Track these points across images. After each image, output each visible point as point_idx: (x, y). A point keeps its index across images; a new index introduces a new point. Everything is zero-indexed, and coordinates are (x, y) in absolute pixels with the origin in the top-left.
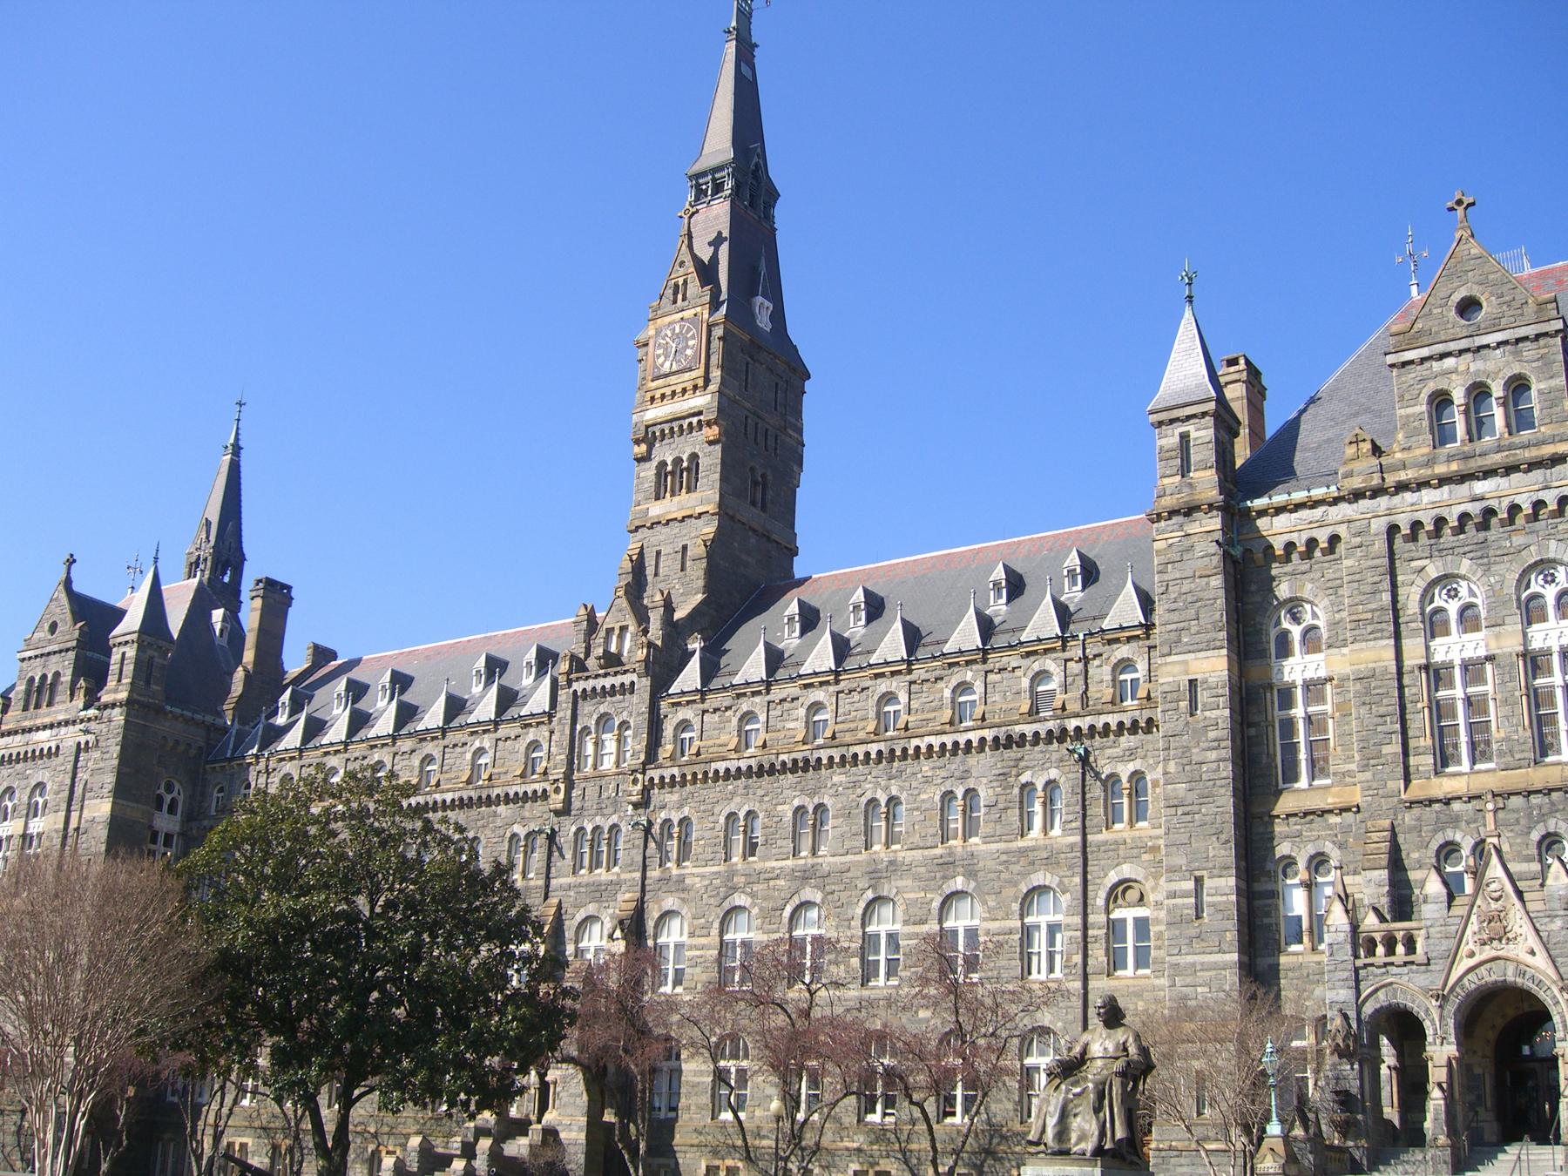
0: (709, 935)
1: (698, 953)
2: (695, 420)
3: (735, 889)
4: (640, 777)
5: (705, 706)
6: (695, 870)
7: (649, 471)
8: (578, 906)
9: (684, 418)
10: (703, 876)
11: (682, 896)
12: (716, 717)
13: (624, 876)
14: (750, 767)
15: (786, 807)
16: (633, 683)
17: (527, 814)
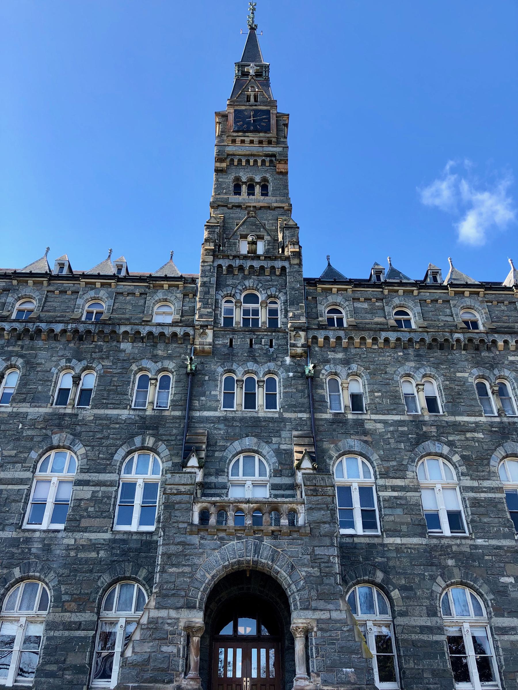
0: (404, 478)
1: (395, 494)
2: (268, 159)
3: (423, 437)
4: (302, 334)
5: (357, 295)
6: (374, 417)
7: (229, 179)
8: (231, 438)
9: (259, 156)
10: (385, 422)
11: (365, 438)
12: (366, 305)
13: (287, 415)
14: (423, 340)
15: (466, 375)
16: (283, 269)
17: (160, 353)
